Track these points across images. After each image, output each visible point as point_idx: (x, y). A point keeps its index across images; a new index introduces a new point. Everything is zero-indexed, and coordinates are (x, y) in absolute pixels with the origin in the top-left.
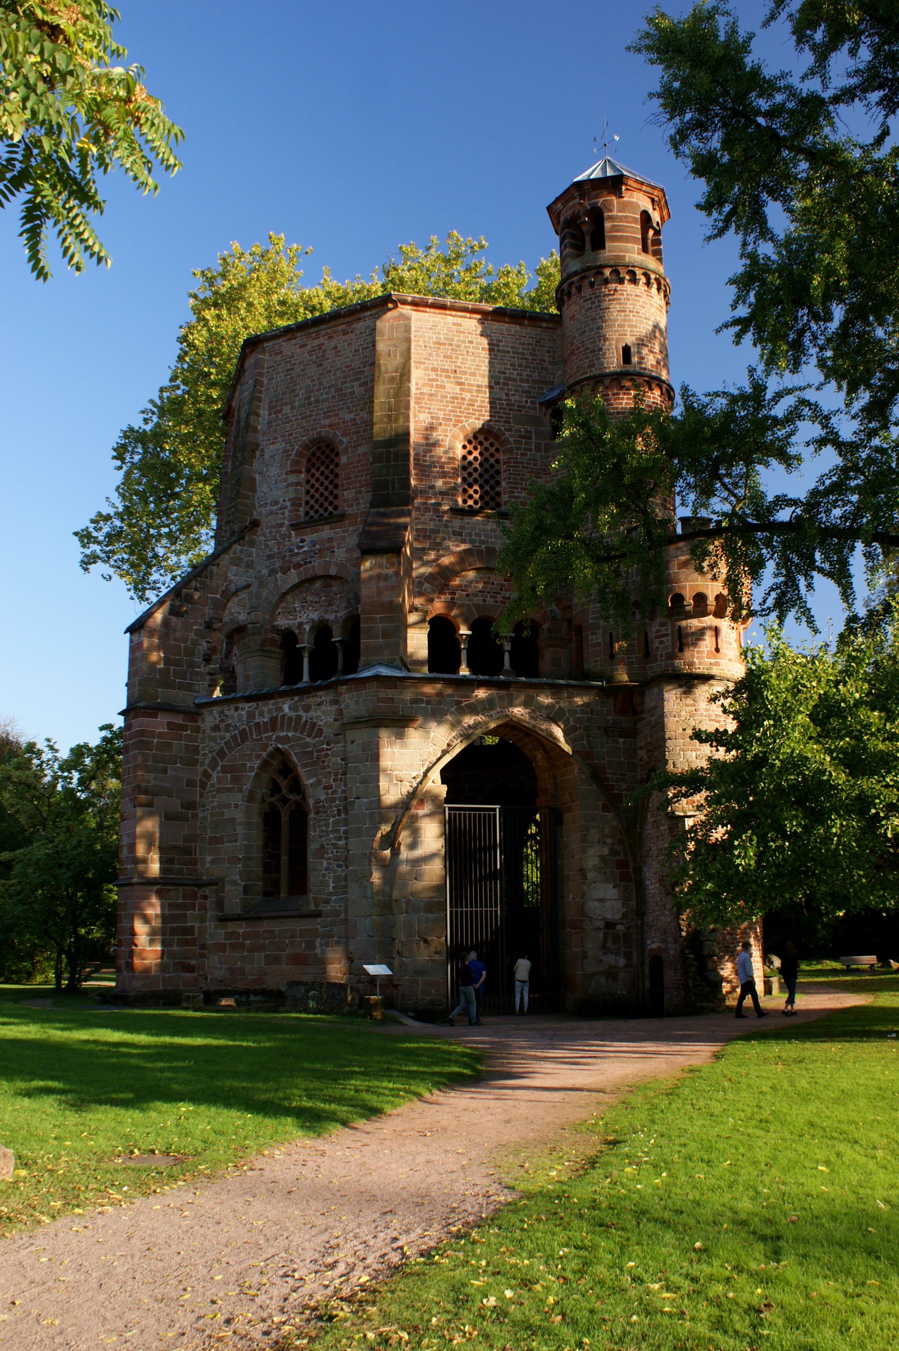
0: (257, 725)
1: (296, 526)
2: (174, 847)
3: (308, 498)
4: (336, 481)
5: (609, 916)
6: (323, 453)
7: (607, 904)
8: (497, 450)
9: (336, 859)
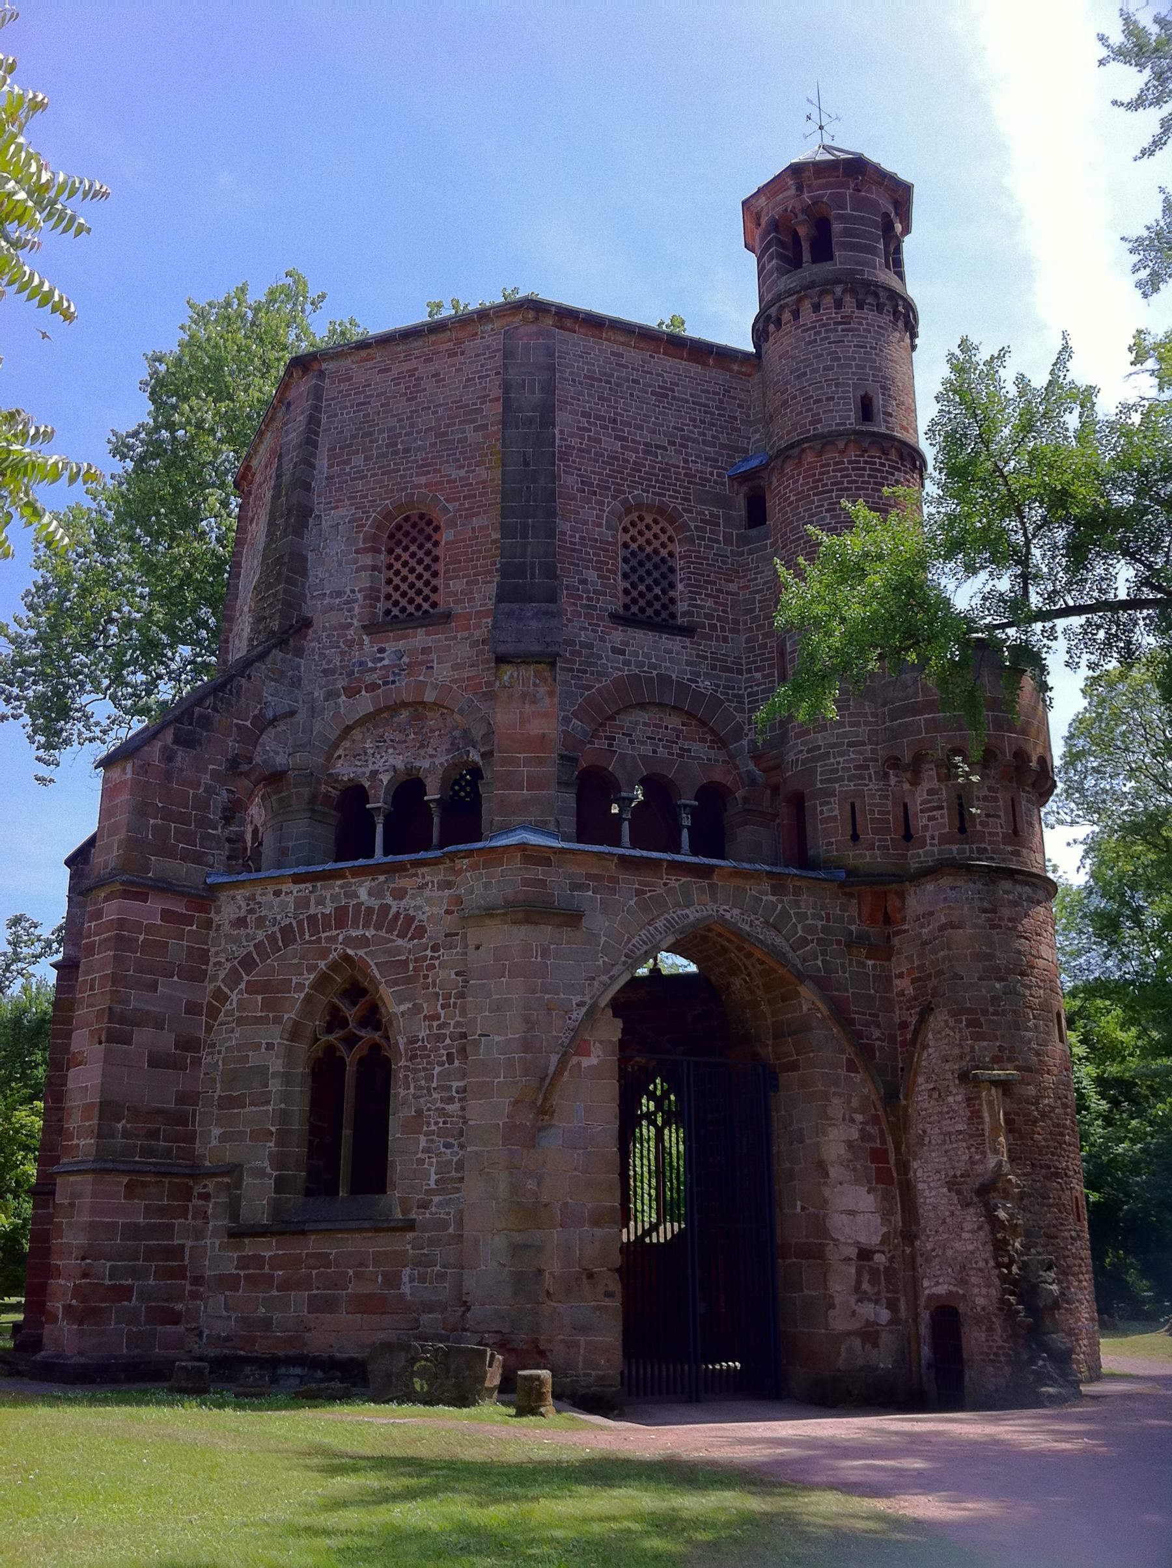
0: (312, 919)
1: (372, 628)
2: (159, 1112)
3: (390, 589)
4: (434, 567)
5: (863, 1239)
6: (414, 526)
7: (860, 1219)
8: (671, 539)
9: (444, 1133)
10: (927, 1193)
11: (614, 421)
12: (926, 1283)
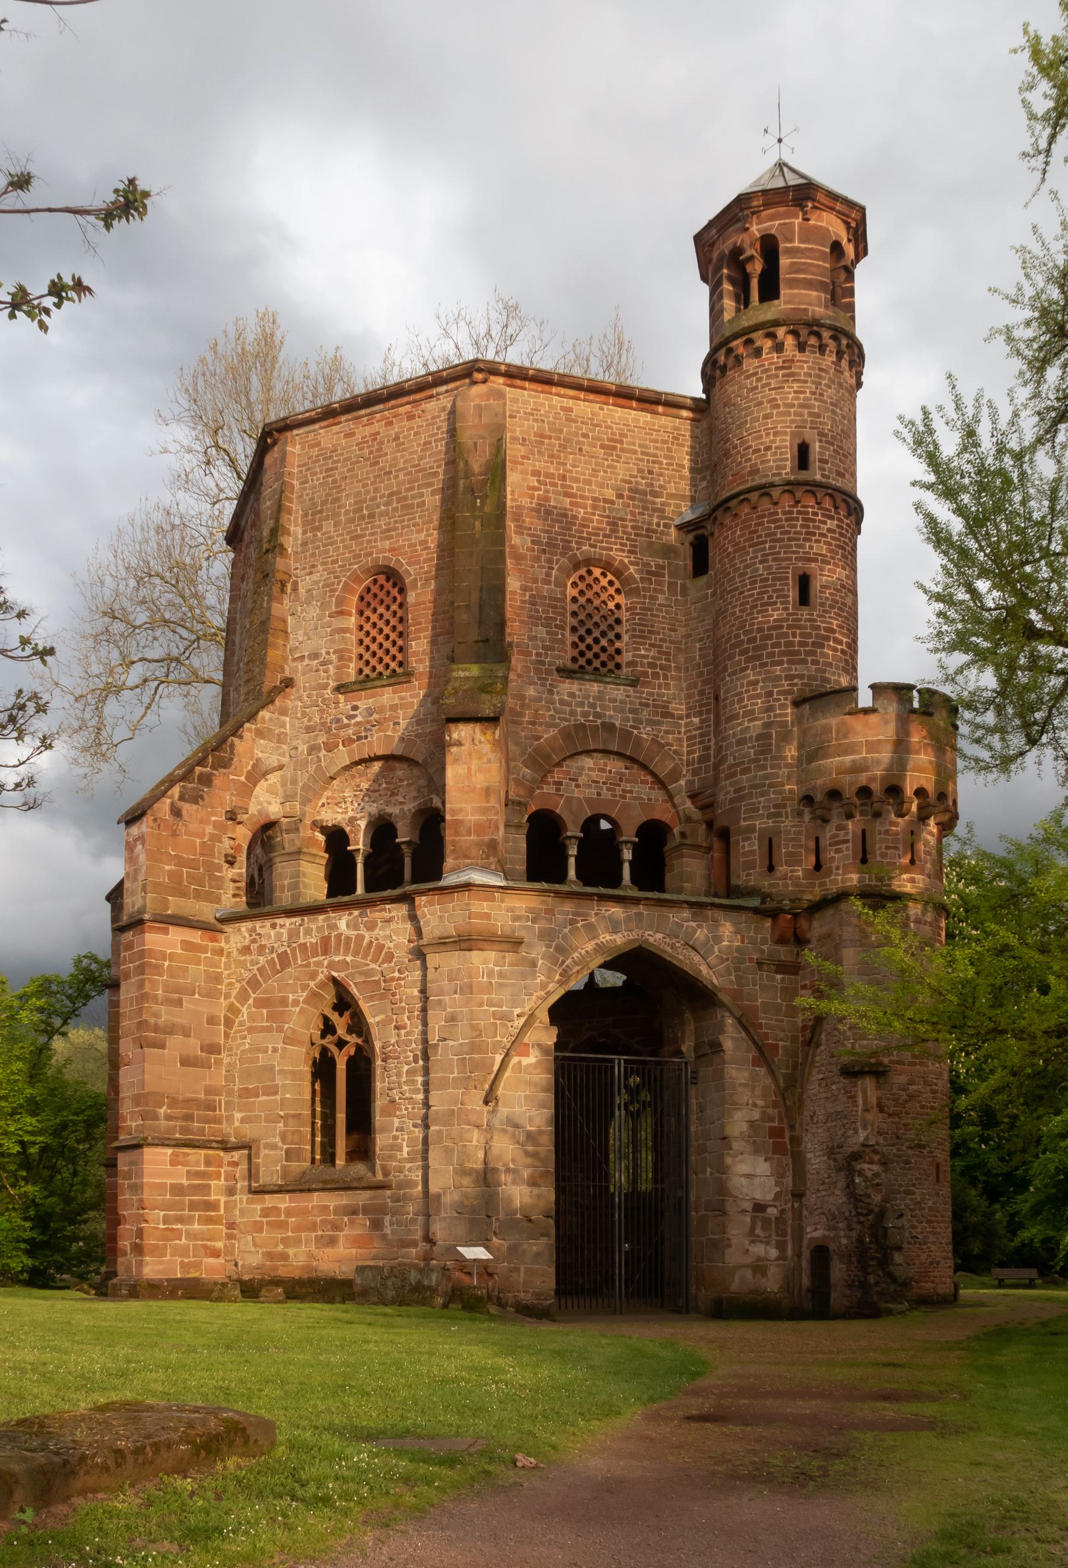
5: (758, 1196)
10: (813, 1161)
11: (564, 478)
12: (809, 1230)
